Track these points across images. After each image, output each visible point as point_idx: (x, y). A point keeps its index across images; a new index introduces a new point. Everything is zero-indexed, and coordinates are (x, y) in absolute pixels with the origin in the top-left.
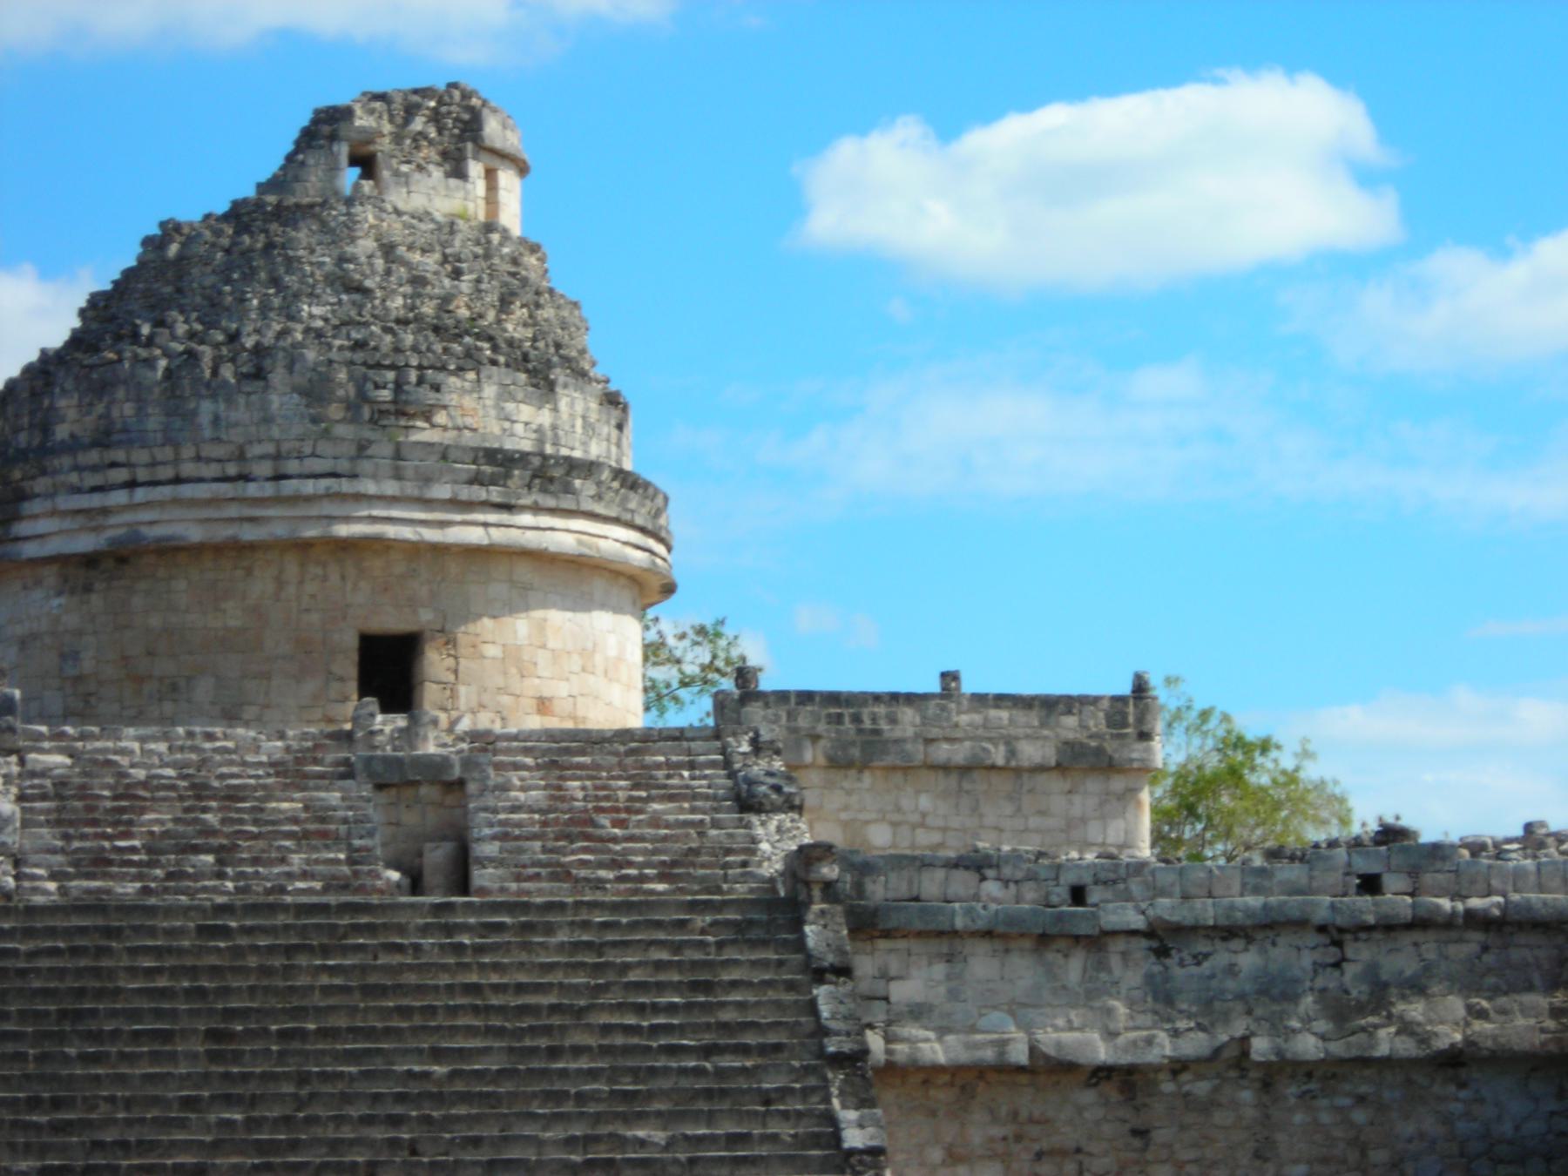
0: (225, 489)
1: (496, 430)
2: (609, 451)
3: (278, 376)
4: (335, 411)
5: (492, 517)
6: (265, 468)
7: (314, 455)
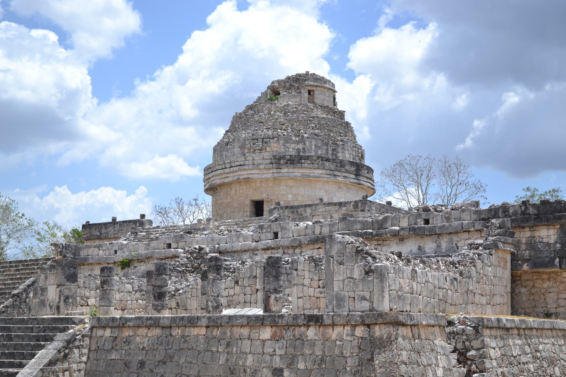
0: (221, 171)
1: (283, 151)
2: (327, 153)
3: (236, 144)
5: (275, 171)
6: (228, 166)
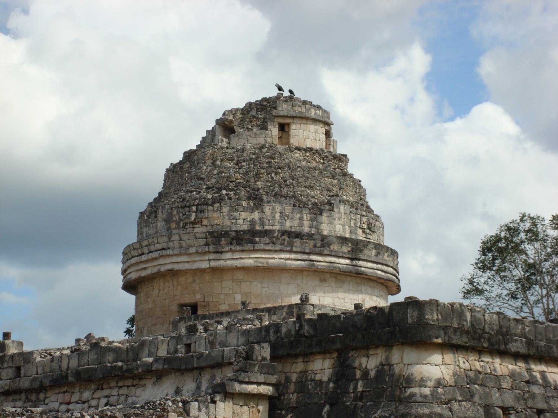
4: (173, 226)
5: (212, 256)
7: (158, 243)
